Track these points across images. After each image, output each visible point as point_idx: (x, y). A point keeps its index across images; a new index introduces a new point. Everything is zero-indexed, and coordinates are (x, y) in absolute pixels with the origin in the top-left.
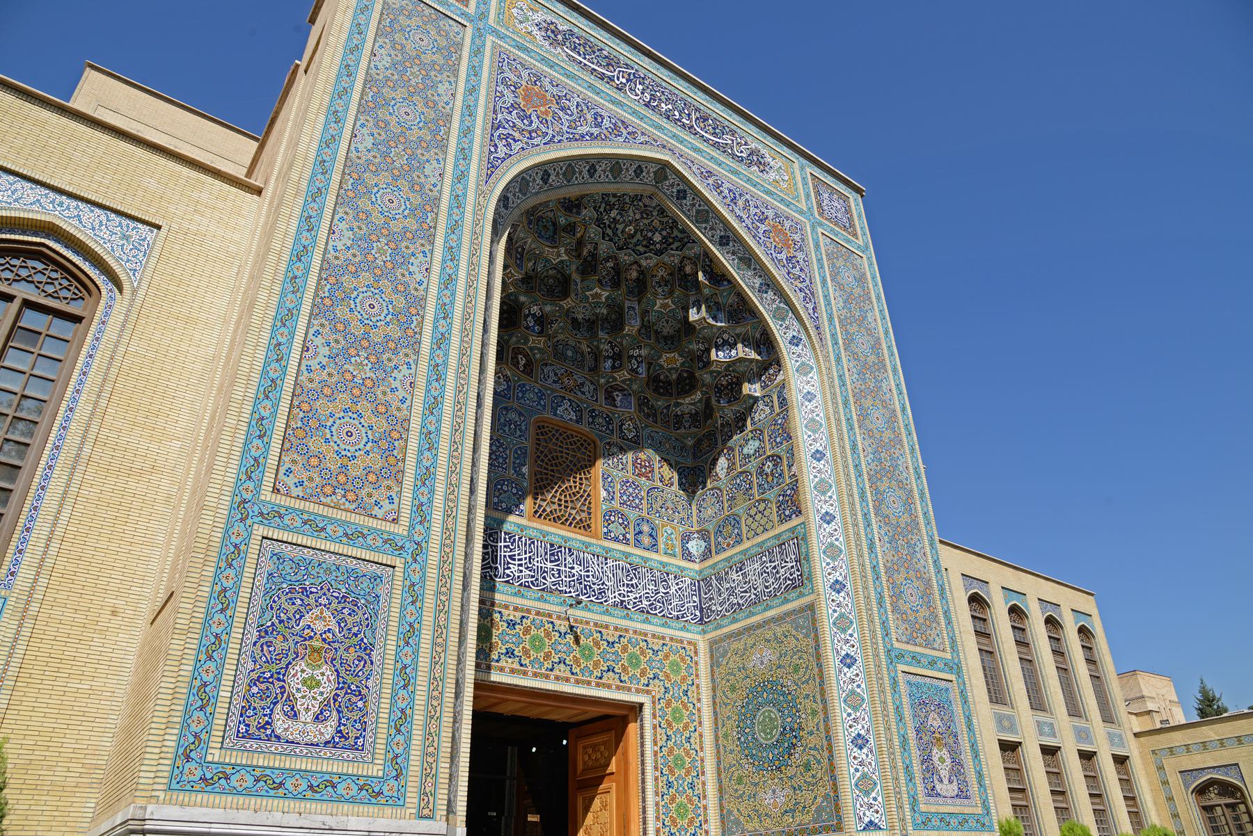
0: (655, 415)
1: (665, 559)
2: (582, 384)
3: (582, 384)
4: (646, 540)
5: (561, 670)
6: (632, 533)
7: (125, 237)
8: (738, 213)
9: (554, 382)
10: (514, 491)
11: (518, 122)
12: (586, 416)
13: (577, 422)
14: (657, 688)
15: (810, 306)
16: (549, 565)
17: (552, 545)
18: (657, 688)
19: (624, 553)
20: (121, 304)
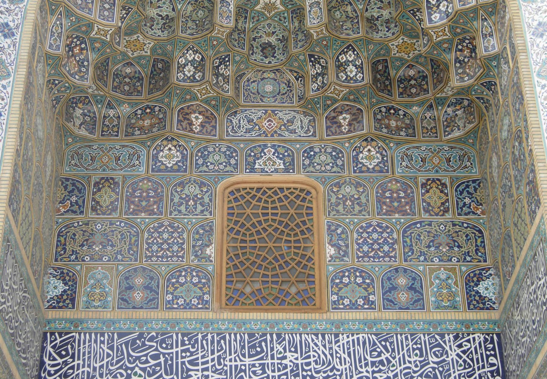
0: (411, 127)
1: (438, 316)
2: (291, 121)
3: (291, 121)
4: (403, 297)
6: (379, 291)
9: (248, 131)
10: (195, 280)
12: (300, 160)
13: (286, 170)
16: (248, 361)
17: (251, 335)
19: (365, 322)
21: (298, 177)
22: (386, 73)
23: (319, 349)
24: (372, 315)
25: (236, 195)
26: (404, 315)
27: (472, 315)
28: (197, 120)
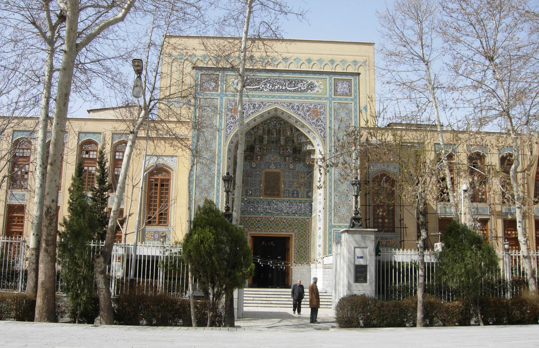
1: (301, 199)
4: (295, 195)
5: (271, 230)
7: (172, 161)
8: (299, 112)
11: (233, 121)
14: (296, 231)
15: (322, 134)
18: (296, 231)
20: (174, 172)
21: (278, 170)
22: (296, 149)
23: (280, 205)
24: (289, 199)
25: (266, 173)
26: (295, 199)
27: (307, 199)
28: (259, 157)
